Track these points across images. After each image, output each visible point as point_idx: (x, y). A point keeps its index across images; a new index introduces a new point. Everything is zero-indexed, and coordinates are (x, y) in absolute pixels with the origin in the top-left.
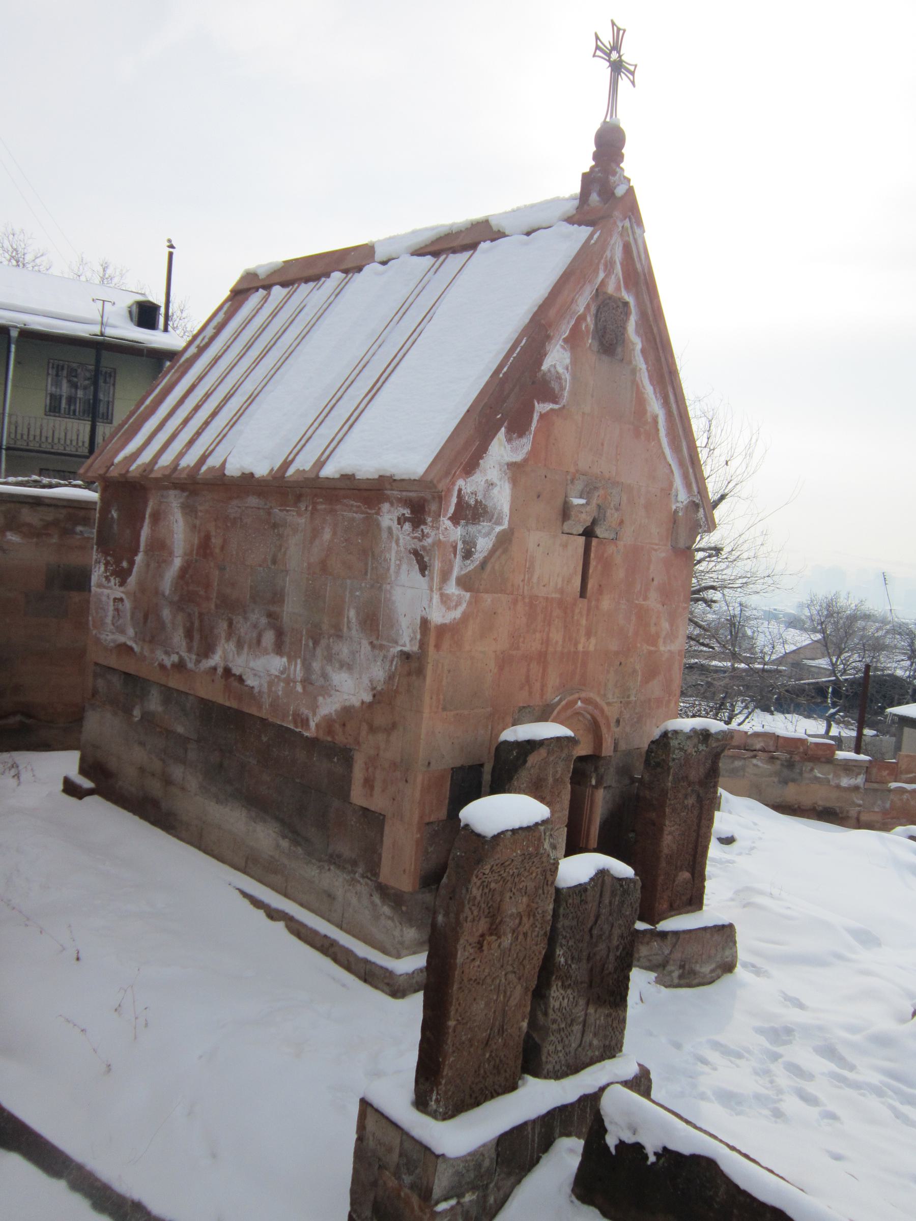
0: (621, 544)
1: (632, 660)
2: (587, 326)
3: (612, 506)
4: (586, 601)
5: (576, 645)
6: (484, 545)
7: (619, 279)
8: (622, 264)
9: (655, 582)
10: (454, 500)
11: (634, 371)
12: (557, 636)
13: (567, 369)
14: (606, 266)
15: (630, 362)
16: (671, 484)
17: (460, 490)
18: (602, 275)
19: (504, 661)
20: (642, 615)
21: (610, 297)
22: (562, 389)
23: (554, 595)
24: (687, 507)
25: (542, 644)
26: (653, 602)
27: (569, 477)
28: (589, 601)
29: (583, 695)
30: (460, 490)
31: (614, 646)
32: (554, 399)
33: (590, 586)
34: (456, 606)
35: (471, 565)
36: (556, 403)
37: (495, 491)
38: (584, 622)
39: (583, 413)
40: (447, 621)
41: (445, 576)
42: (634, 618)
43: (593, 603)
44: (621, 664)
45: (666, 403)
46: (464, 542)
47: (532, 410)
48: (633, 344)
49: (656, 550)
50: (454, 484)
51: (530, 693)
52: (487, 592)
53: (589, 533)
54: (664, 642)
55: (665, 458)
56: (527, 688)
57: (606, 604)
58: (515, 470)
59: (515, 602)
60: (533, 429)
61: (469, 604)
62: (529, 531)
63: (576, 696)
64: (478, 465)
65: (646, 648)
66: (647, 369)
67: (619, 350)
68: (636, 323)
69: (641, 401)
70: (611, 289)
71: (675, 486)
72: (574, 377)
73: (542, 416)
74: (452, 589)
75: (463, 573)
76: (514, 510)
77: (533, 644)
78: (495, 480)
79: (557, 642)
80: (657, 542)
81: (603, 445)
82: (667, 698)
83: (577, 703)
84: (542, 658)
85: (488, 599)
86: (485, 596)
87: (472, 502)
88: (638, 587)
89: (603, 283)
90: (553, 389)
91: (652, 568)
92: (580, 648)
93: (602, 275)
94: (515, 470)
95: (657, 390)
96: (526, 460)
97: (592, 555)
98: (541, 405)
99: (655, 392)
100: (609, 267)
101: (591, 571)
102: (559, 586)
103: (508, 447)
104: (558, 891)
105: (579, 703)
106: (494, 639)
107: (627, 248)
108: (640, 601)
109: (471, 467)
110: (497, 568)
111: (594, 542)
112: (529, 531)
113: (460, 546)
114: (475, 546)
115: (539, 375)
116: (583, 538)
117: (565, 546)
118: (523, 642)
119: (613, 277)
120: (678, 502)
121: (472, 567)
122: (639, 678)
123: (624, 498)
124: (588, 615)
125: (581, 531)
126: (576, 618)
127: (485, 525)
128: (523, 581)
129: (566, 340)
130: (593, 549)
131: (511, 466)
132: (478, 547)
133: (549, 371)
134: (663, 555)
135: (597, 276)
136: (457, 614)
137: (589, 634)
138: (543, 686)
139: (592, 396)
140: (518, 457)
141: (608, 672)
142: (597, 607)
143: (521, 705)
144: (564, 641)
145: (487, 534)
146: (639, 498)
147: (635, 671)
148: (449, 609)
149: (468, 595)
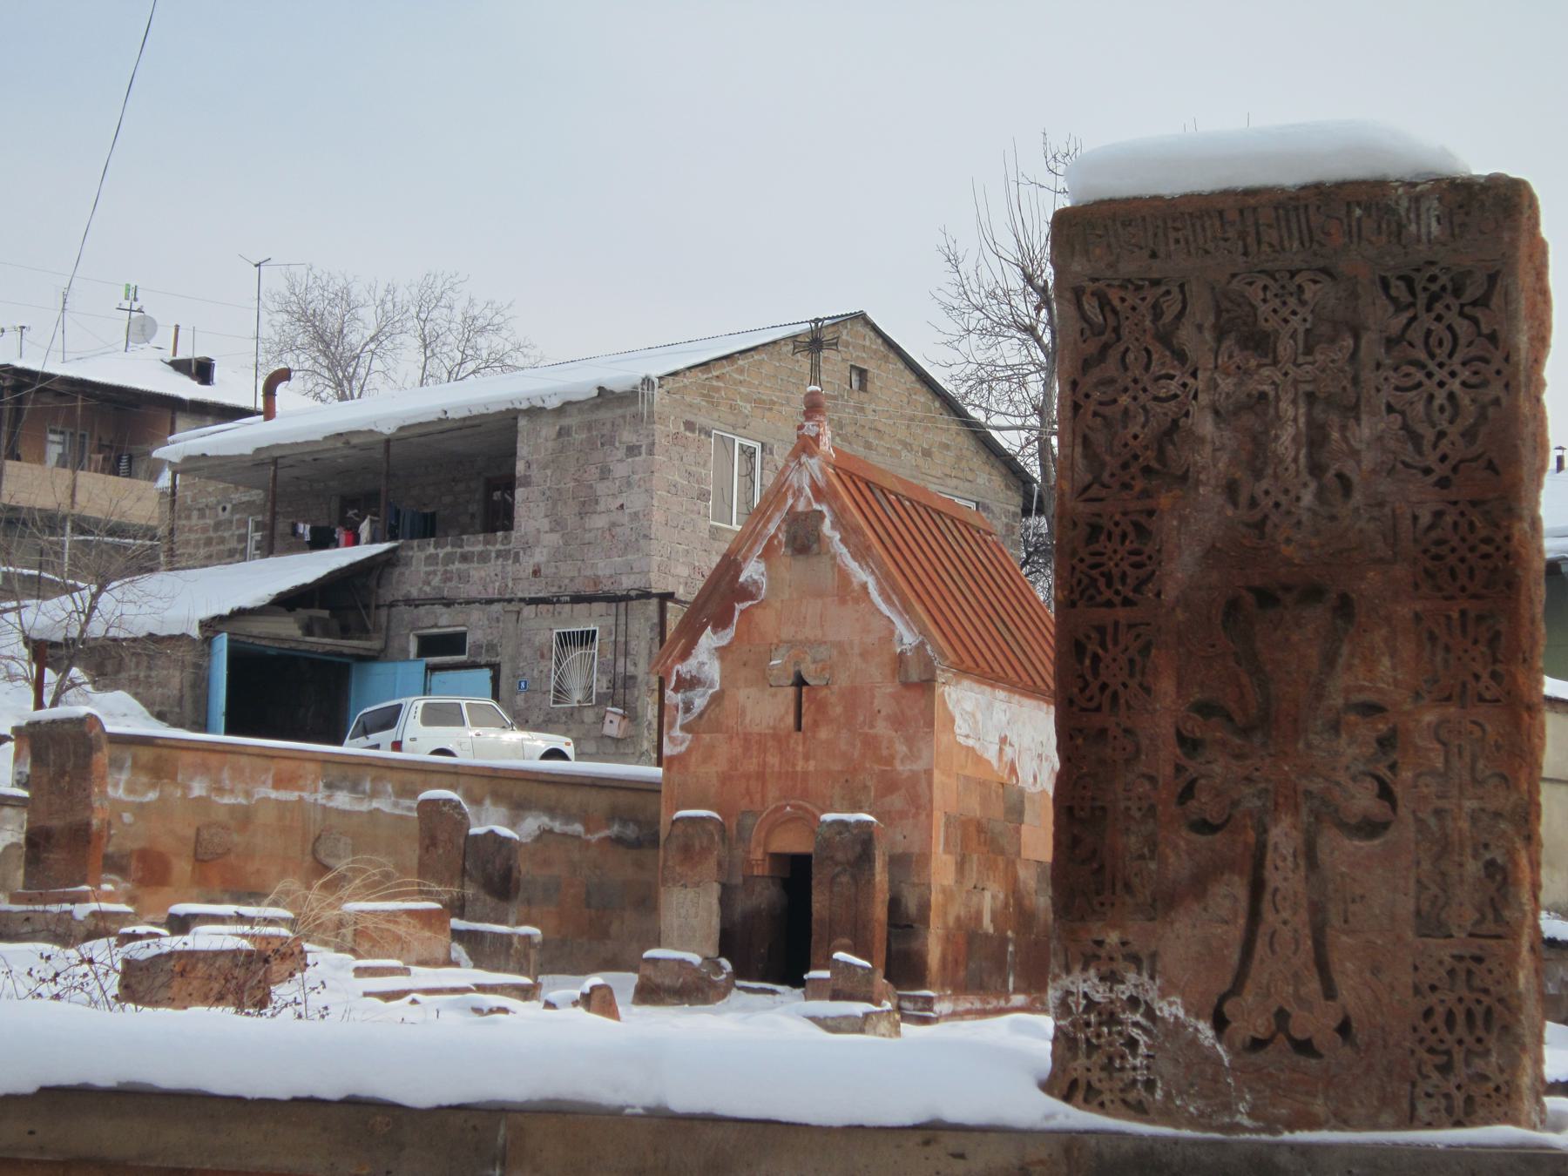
0: (835, 688)
1: (861, 777)
2: (780, 542)
3: (809, 658)
4: (800, 734)
5: (794, 765)
6: (699, 703)
7: (809, 499)
8: (810, 487)
9: (883, 713)
10: (674, 678)
11: (834, 558)
12: (773, 760)
13: (763, 574)
14: (794, 493)
15: (829, 551)
16: (892, 632)
17: (678, 672)
18: (790, 502)
19: (725, 779)
20: (871, 743)
21: (802, 513)
22: (759, 589)
23: (767, 731)
24: (917, 647)
25: (759, 765)
26: (882, 729)
27: (773, 647)
28: (804, 733)
29: (792, 802)
30: (678, 672)
31: (836, 766)
32: (752, 597)
33: (804, 721)
34: (681, 744)
35: (690, 717)
36: (753, 599)
37: (706, 667)
38: (800, 749)
39: (782, 601)
40: (675, 753)
41: (671, 726)
42: (858, 744)
43: (809, 734)
44: (847, 781)
45: (873, 572)
46: (684, 703)
47: (733, 609)
48: (829, 538)
49: (879, 687)
50: (672, 668)
51: (752, 801)
52: (704, 732)
53: (800, 682)
54: (902, 761)
55: (881, 613)
56: (748, 798)
57: (823, 734)
58: (722, 652)
59: (731, 738)
60: (735, 621)
61: (692, 741)
62: (738, 688)
63: (784, 803)
64: (690, 654)
65: (877, 768)
66: (849, 551)
67: (815, 546)
68: (831, 522)
69: (844, 576)
70: (801, 507)
71: (897, 632)
72: (770, 579)
73: (742, 612)
74: (677, 733)
75: (686, 721)
76: (723, 678)
77: (752, 765)
78: (705, 660)
79: (773, 766)
80: (880, 680)
81: (805, 618)
82: (913, 810)
83: (785, 807)
84: (761, 776)
85: (707, 738)
86: (704, 736)
87: (688, 677)
88: (861, 718)
89: (792, 506)
90: (751, 592)
91: (876, 702)
92: (799, 768)
93: (790, 502)
94: (722, 652)
95: (863, 563)
96: (731, 644)
97: (804, 699)
98: (741, 605)
99: (860, 565)
100: (798, 493)
101: (803, 711)
102: (771, 724)
103: (715, 638)
104: (467, 837)
105: (788, 808)
106: (716, 764)
107: (811, 476)
108: (866, 729)
109: (685, 655)
110: (712, 716)
111: (805, 689)
112: (738, 688)
113: (681, 705)
114: (693, 704)
115: (737, 586)
116: (793, 688)
117: (774, 695)
118: (741, 765)
119: (802, 499)
120: (903, 644)
121: (691, 718)
122: (872, 794)
123: (835, 653)
124: (804, 743)
125: (790, 682)
126: (791, 746)
127: (700, 690)
128: (737, 723)
129: (759, 557)
130: (803, 695)
131: (717, 649)
132: (696, 705)
133: (746, 580)
134: (889, 690)
135: (785, 505)
136: (682, 748)
137: (807, 758)
138: (763, 797)
139: (790, 586)
140: (724, 642)
141: (833, 787)
142: (814, 738)
143: (743, 809)
144: (781, 763)
145: (703, 695)
146: (852, 649)
147: (865, 787)
148: (676, 745)
149: (690, 736)
